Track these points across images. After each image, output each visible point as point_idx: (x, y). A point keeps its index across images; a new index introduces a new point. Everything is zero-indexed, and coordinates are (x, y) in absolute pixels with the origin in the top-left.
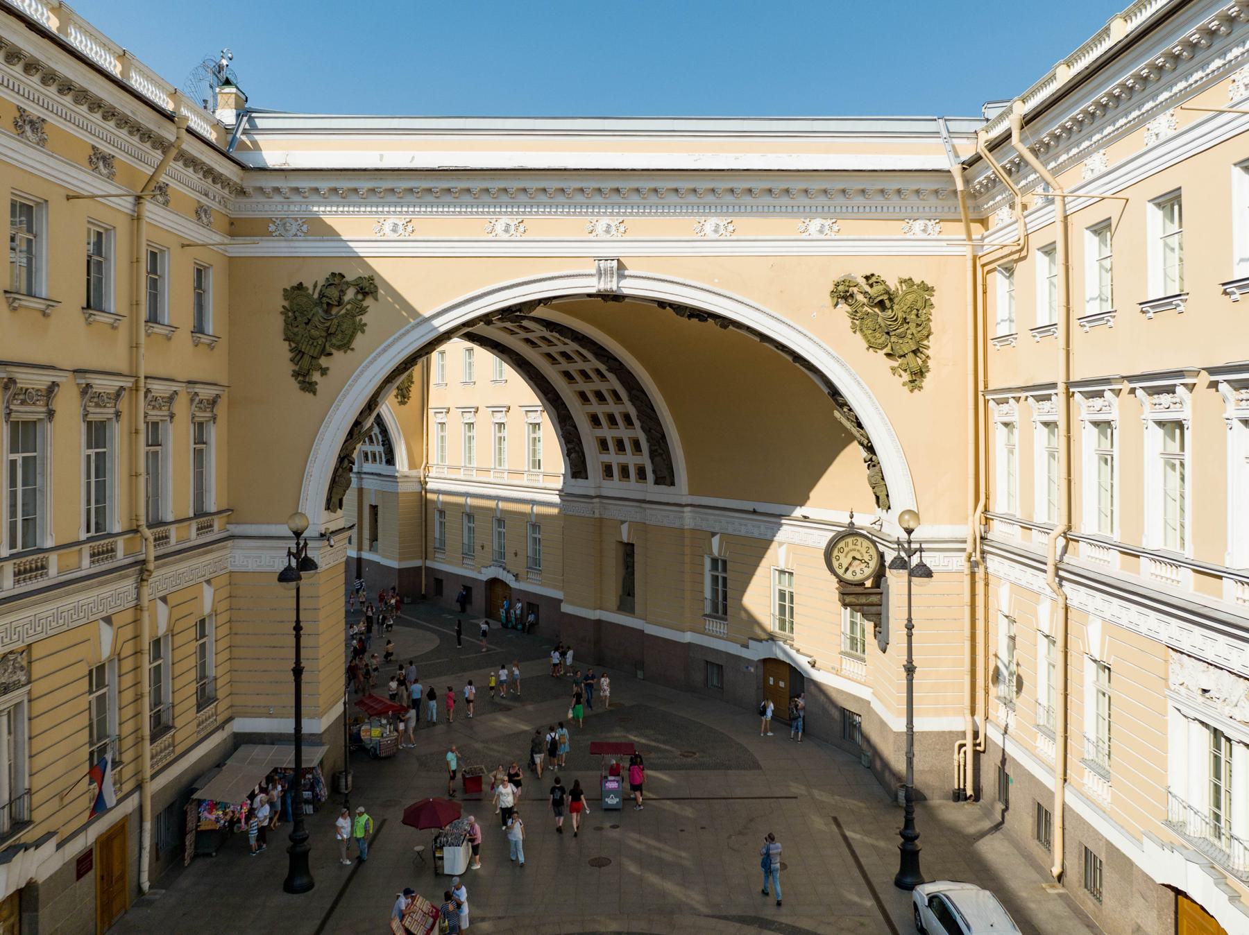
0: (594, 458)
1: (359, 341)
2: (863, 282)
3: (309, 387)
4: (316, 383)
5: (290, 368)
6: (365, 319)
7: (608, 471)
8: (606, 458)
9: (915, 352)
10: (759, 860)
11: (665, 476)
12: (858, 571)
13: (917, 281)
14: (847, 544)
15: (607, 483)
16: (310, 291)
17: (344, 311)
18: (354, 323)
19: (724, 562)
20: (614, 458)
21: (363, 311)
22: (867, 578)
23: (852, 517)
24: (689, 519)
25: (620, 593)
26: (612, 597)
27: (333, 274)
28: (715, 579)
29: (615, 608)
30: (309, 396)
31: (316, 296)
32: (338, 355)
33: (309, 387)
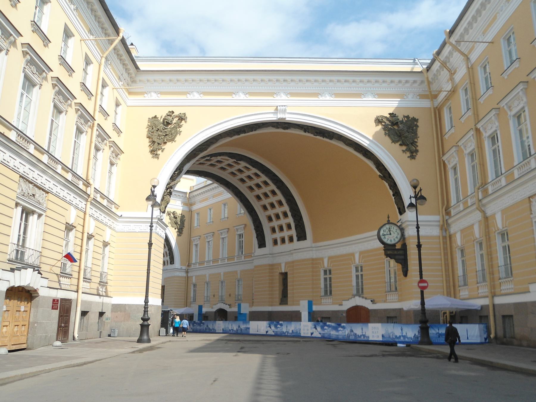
1: (178, 138)
2: (388, 116)
3: (156, 156)
5: (148, 149)
6: (181, 129)
7: (275, 242)
8: (275, 236)
9: (412, 144)
11: (302, 236)
12: (393, 240)
13: (411, 116)
15: (276, 247)
16: (159, 119)
19: (330, 271)
21: (180, 127)
23: (388, 218)
24: (314, 254)
25: (281, 297)
26: (278, 300)
29: (278, 303)
30: (156, 160)
31: (162, 121)
32: (169, 144)
33: (156, 156)
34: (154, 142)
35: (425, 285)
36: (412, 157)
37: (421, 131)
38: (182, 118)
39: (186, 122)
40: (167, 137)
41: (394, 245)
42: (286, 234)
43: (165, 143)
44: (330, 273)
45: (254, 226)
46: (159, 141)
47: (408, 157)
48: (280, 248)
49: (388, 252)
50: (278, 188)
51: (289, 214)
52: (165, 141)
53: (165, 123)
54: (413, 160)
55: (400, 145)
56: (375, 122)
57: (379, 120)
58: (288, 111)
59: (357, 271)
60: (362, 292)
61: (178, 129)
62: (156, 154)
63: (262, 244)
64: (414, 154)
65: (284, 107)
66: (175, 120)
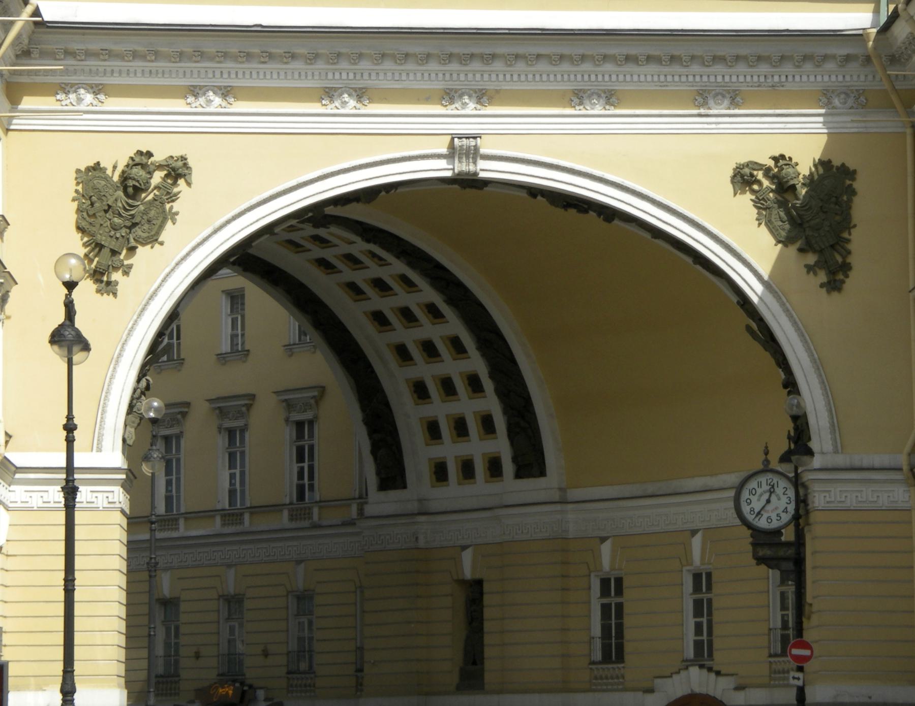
0: (418, 454)
1: (169, 232)
4: (117, 283)
6: (176, 206)
7: (440, 472)
8: (438, 451)
10: (560, 212)
11: (530, 462)
12: (774, 517)
13: (837, 162)
14: (760, 485)
16: (109, 172)
17: (151, 197)
18: (164, 211)
19: (619, 581)
20: (450, 450)
21: (173, 198)
22: (786, 525)
23: (766, 453)
27: (140, 153)
28: (606, 609)
31: (116, 178)
34: (99, 246)
35: (806, 652)
36: (834, 285)
37: (863, 209)
38: (177, 171)
39: (189, 184)
40: (138, 231)
41: (777, 532)
42: (477, 447)
43: (132, 250)
44: (619, 591)
45: (363, 409)
46: (113, 245)
47: (822, 286)
48: (454, 492)
49: (766, 552)
50: (450, 301)
51: (488, 385)
52: (133, 243)
53: (130, 190)
54: (835, 294)
55: (801, 250)
56: (733, 182)
57: (742, 176)
58: (483, 151)
59: (697, 588)
60: (710, 654)
61: (168, 206)
62: (109, 283)
63: (392, 475)
64: (840, 276)
65: (472, 142)
66: (158, 177)
